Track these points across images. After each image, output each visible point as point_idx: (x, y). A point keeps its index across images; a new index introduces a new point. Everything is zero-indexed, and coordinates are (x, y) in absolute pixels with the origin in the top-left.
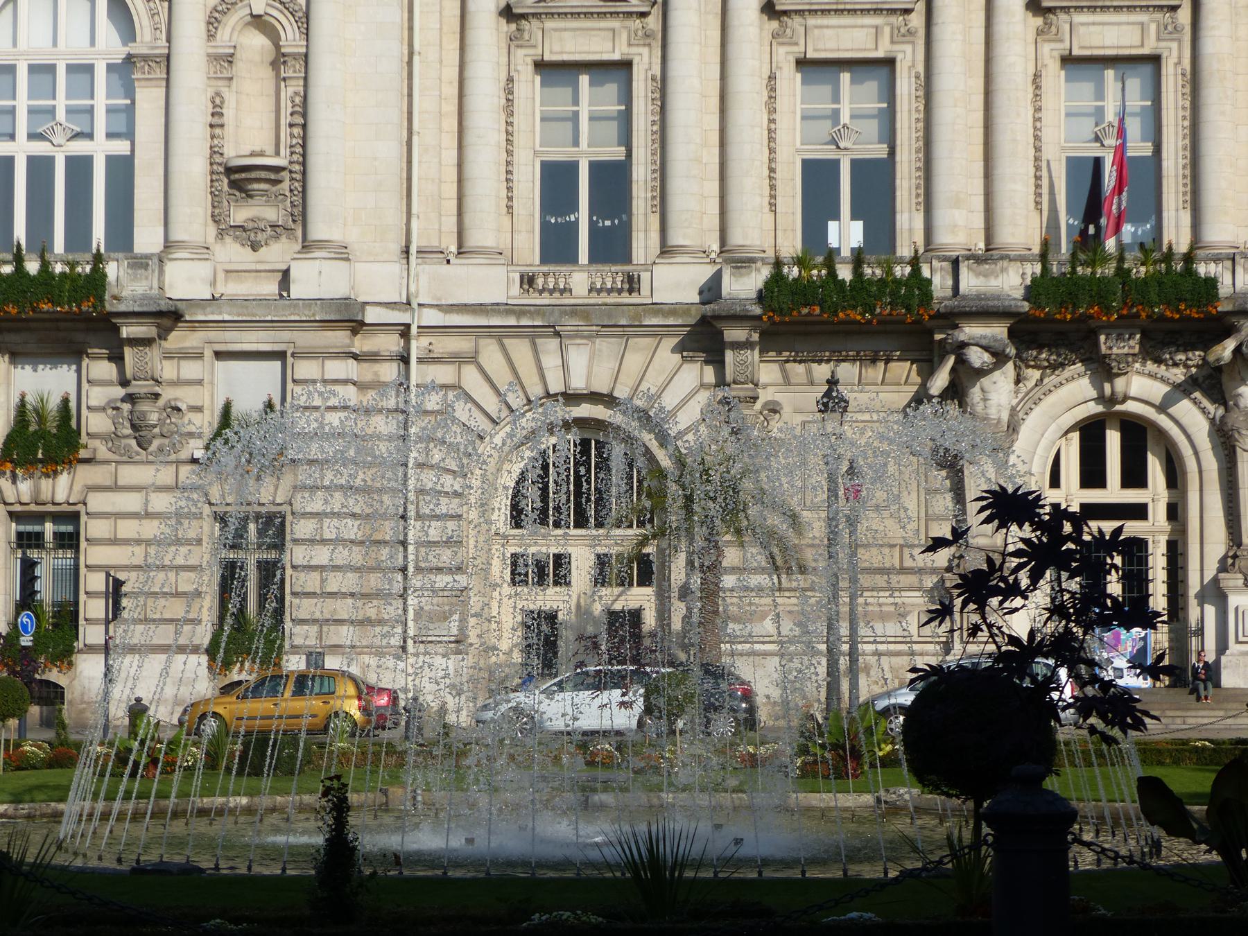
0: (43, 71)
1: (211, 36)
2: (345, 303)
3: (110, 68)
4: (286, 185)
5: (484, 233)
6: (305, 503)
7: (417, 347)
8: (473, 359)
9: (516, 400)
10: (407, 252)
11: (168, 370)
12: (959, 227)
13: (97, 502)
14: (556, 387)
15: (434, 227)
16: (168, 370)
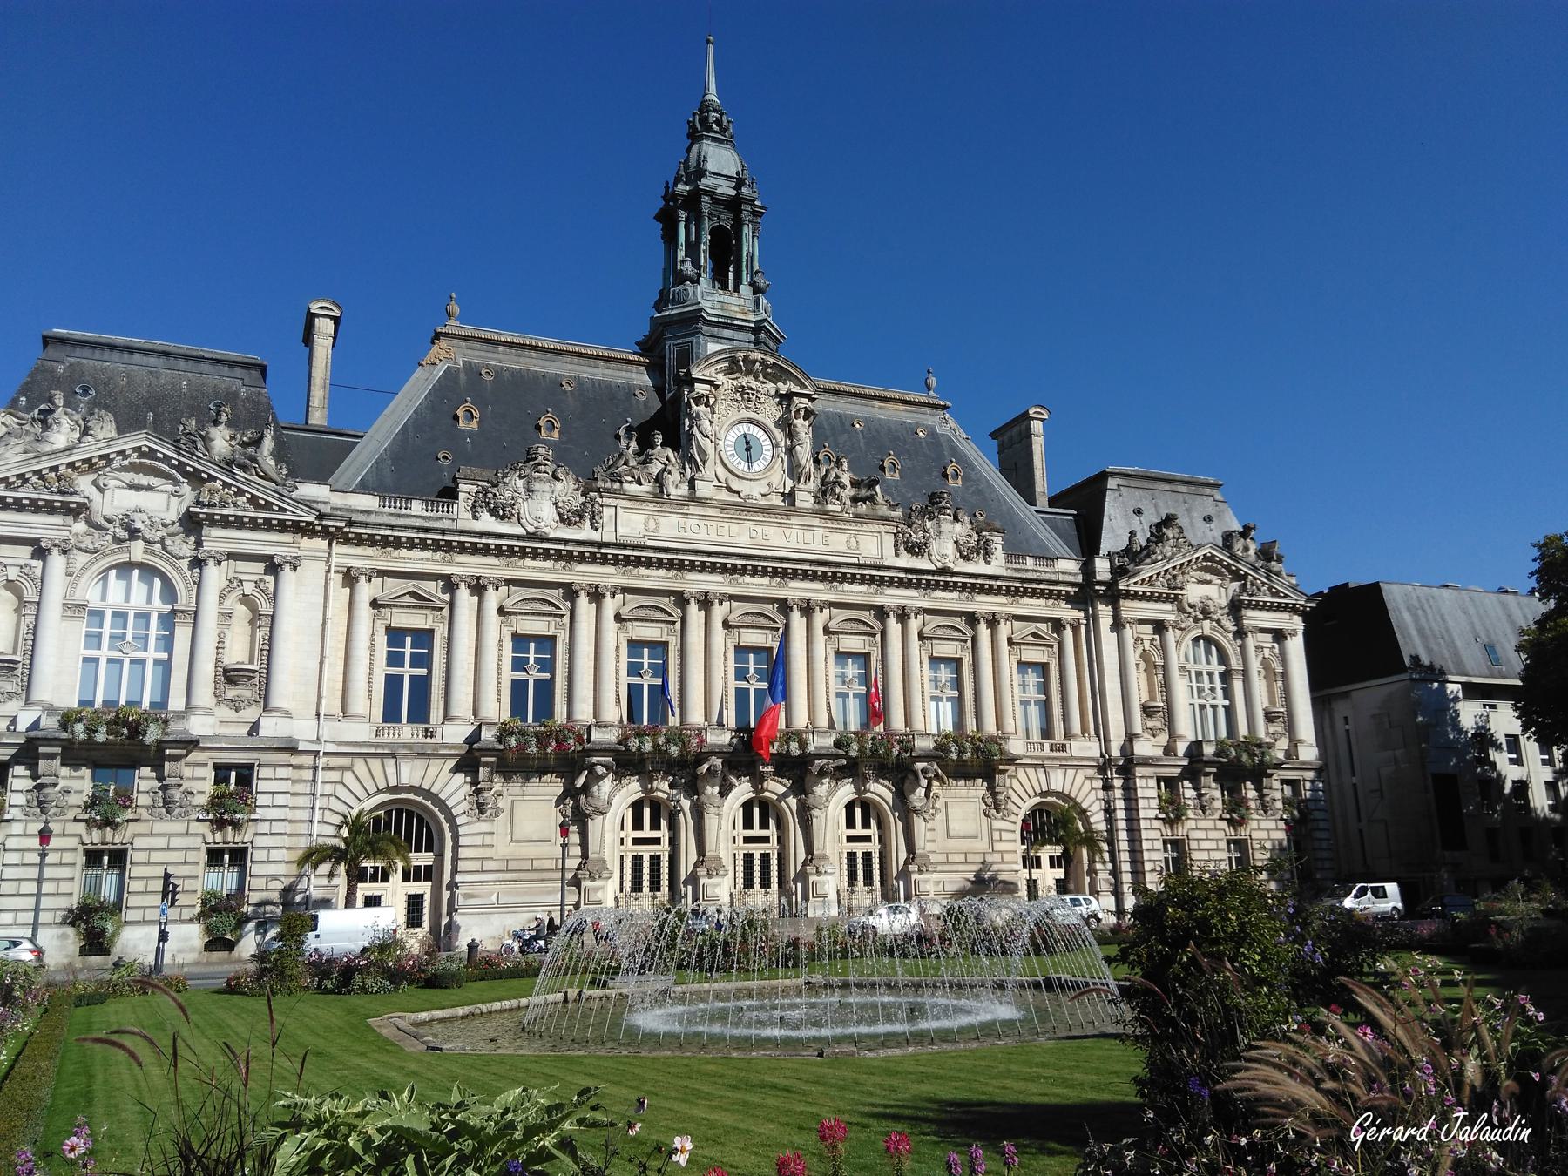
0: (120, 616)
1: (221, 603)
2: (290, 739)
3: (160, 616)
4: (256, 680)
5: (359, 704)
6: (259, 841)
7: (322, 762)
8: (350, 769)
9: (372, 789)
10: (318, 715)
11: (187, 772)
12: (584, 714)
13: (138, 843)
14: (393, 783)
15: (332, 703)
16: (187, 772)
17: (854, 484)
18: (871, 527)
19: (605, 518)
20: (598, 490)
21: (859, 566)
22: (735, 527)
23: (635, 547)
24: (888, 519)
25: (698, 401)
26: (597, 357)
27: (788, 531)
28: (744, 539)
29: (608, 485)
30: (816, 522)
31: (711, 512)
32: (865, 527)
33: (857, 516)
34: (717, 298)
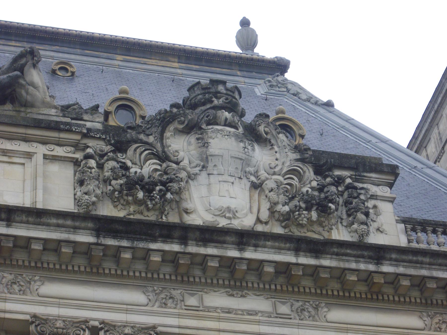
24: (55, 127)
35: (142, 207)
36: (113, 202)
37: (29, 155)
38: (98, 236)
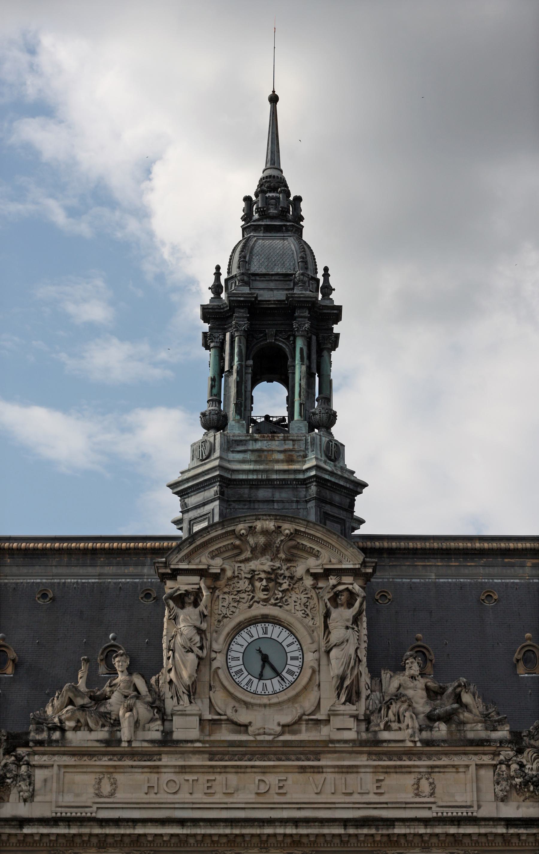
17: (432, 694)
18: (457, 761)
19: (38, 784)
20: (26, 745)
21: (426, 822)
22: (233, 779)
23: (69, 821)
24: (481, 742)
25: (181, 600)
26: (94, 551)
27: (319, 778)
28: (246, 796)
29: (44, 736)
30: (362, 761)
31: (195, 761)
32: (445, 761)
33: (427, 743)
34: (252, 446)
35: (533, 794)
36: (516, 791)
37: (467, 766)
38: (507, 828)
